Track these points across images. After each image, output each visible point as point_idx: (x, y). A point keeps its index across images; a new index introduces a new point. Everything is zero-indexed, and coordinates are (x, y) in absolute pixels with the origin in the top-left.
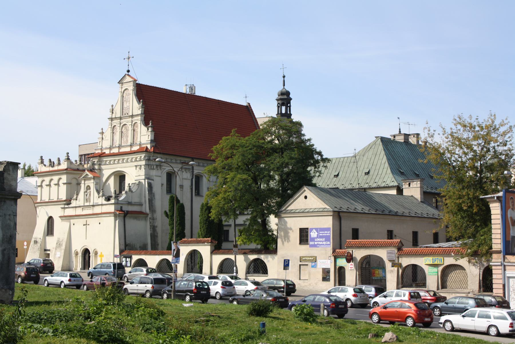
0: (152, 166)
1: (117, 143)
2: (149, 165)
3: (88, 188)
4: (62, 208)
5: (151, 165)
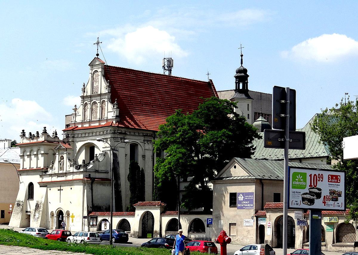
0: (117, 139)
1: (88, 118)
2: (114, 138)
3: (62, 158)
5: (116, 138)
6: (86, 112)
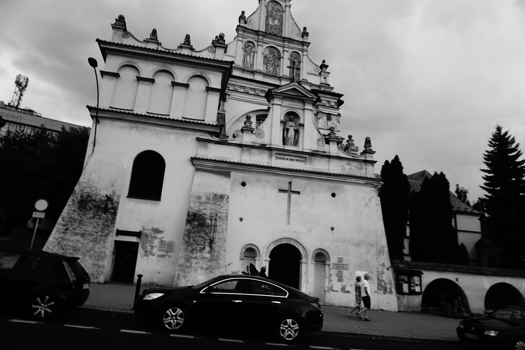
4: (198, 139)
6: (248, 57)
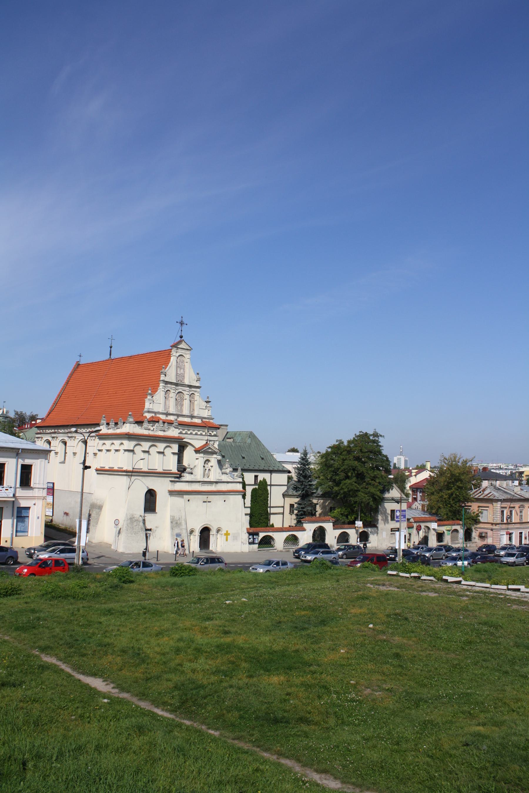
4: (171, 481)
